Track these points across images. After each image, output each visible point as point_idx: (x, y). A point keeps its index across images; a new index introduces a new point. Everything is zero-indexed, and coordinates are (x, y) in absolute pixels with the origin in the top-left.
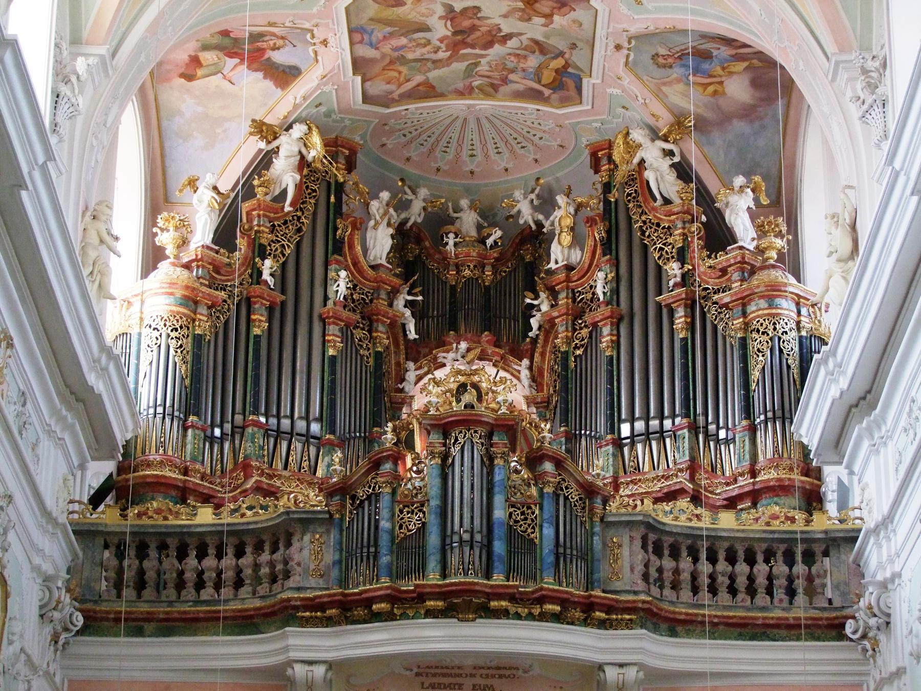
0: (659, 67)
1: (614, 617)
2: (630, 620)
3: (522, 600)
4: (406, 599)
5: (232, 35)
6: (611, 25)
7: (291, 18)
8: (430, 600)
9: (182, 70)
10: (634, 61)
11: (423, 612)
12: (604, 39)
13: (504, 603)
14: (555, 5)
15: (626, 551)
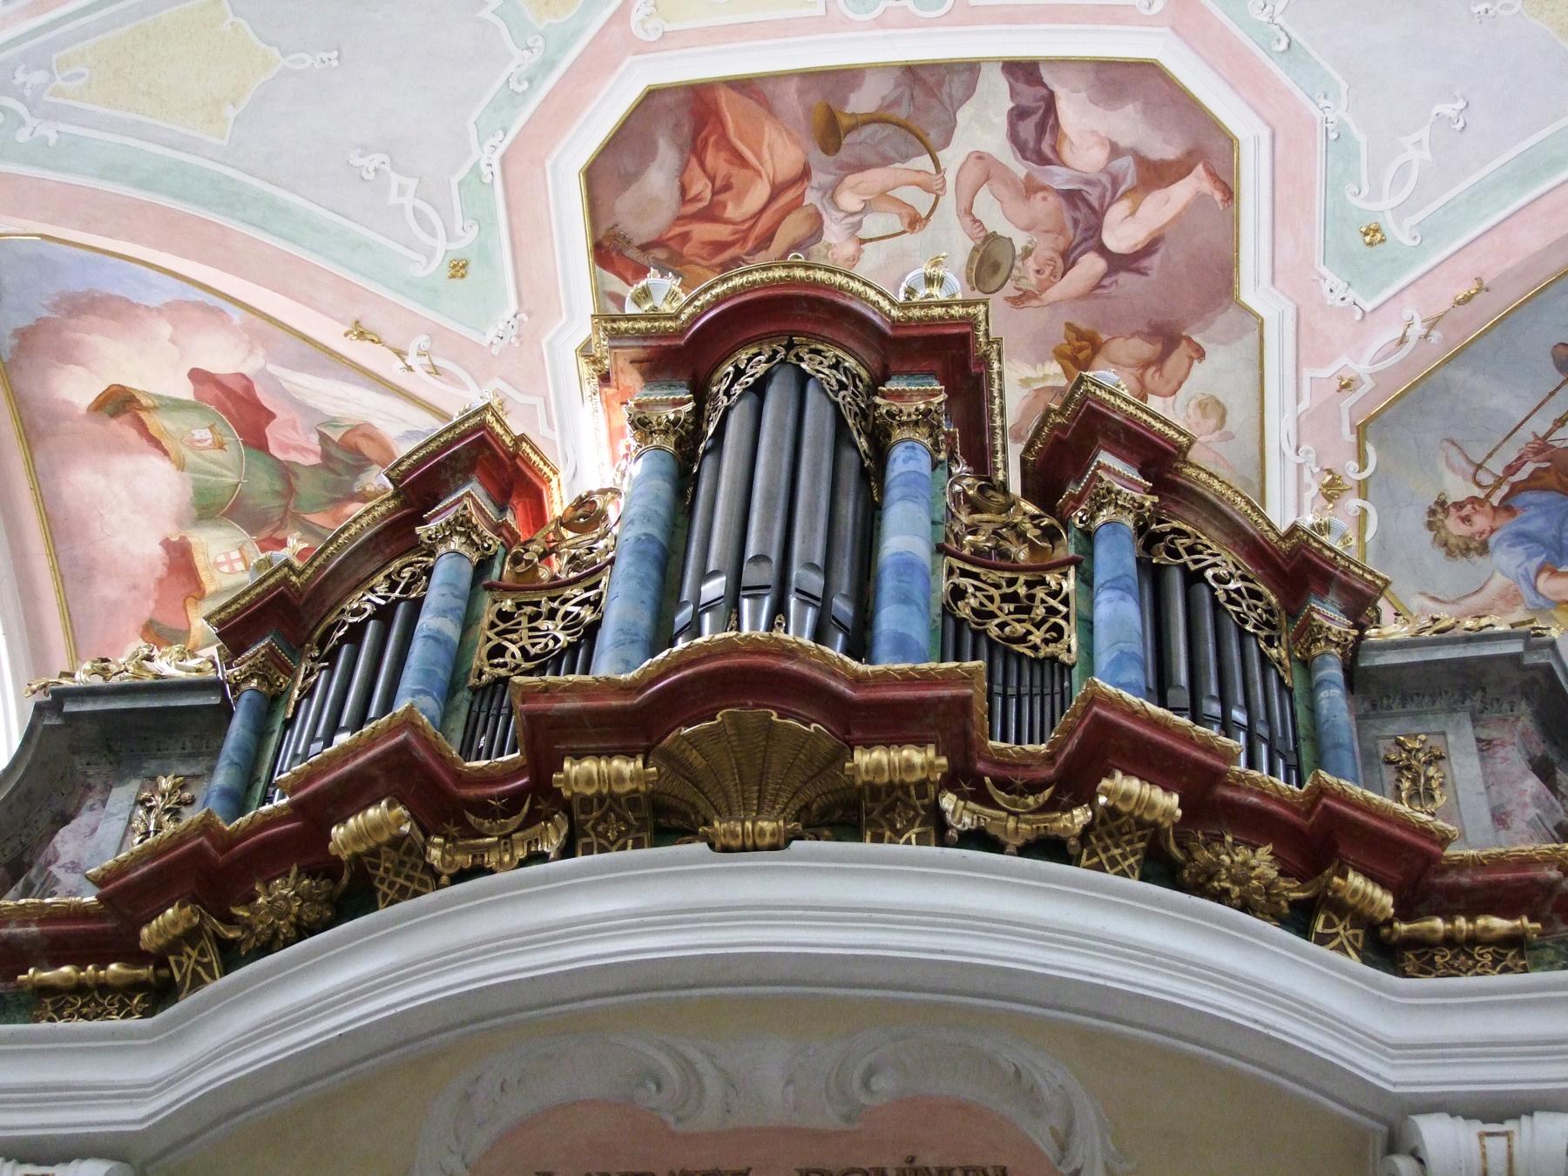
0: (1450, 554)
1: (1439, 923)
2: (1515, 941)
3: (1002, 784)
4: (482, 808)
5: (273, 433)
6: (1307, 373)
7: (422, 341)
8: (579, 756)
9: (147, 610)
10: (1381, 537)
11: (550, 845)
12: (1290, 452)
13: (915, 755)
14: (1146, 349)
15: (1464, 767)
